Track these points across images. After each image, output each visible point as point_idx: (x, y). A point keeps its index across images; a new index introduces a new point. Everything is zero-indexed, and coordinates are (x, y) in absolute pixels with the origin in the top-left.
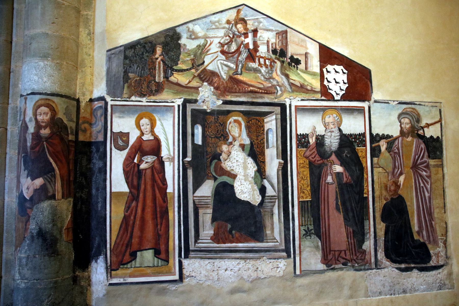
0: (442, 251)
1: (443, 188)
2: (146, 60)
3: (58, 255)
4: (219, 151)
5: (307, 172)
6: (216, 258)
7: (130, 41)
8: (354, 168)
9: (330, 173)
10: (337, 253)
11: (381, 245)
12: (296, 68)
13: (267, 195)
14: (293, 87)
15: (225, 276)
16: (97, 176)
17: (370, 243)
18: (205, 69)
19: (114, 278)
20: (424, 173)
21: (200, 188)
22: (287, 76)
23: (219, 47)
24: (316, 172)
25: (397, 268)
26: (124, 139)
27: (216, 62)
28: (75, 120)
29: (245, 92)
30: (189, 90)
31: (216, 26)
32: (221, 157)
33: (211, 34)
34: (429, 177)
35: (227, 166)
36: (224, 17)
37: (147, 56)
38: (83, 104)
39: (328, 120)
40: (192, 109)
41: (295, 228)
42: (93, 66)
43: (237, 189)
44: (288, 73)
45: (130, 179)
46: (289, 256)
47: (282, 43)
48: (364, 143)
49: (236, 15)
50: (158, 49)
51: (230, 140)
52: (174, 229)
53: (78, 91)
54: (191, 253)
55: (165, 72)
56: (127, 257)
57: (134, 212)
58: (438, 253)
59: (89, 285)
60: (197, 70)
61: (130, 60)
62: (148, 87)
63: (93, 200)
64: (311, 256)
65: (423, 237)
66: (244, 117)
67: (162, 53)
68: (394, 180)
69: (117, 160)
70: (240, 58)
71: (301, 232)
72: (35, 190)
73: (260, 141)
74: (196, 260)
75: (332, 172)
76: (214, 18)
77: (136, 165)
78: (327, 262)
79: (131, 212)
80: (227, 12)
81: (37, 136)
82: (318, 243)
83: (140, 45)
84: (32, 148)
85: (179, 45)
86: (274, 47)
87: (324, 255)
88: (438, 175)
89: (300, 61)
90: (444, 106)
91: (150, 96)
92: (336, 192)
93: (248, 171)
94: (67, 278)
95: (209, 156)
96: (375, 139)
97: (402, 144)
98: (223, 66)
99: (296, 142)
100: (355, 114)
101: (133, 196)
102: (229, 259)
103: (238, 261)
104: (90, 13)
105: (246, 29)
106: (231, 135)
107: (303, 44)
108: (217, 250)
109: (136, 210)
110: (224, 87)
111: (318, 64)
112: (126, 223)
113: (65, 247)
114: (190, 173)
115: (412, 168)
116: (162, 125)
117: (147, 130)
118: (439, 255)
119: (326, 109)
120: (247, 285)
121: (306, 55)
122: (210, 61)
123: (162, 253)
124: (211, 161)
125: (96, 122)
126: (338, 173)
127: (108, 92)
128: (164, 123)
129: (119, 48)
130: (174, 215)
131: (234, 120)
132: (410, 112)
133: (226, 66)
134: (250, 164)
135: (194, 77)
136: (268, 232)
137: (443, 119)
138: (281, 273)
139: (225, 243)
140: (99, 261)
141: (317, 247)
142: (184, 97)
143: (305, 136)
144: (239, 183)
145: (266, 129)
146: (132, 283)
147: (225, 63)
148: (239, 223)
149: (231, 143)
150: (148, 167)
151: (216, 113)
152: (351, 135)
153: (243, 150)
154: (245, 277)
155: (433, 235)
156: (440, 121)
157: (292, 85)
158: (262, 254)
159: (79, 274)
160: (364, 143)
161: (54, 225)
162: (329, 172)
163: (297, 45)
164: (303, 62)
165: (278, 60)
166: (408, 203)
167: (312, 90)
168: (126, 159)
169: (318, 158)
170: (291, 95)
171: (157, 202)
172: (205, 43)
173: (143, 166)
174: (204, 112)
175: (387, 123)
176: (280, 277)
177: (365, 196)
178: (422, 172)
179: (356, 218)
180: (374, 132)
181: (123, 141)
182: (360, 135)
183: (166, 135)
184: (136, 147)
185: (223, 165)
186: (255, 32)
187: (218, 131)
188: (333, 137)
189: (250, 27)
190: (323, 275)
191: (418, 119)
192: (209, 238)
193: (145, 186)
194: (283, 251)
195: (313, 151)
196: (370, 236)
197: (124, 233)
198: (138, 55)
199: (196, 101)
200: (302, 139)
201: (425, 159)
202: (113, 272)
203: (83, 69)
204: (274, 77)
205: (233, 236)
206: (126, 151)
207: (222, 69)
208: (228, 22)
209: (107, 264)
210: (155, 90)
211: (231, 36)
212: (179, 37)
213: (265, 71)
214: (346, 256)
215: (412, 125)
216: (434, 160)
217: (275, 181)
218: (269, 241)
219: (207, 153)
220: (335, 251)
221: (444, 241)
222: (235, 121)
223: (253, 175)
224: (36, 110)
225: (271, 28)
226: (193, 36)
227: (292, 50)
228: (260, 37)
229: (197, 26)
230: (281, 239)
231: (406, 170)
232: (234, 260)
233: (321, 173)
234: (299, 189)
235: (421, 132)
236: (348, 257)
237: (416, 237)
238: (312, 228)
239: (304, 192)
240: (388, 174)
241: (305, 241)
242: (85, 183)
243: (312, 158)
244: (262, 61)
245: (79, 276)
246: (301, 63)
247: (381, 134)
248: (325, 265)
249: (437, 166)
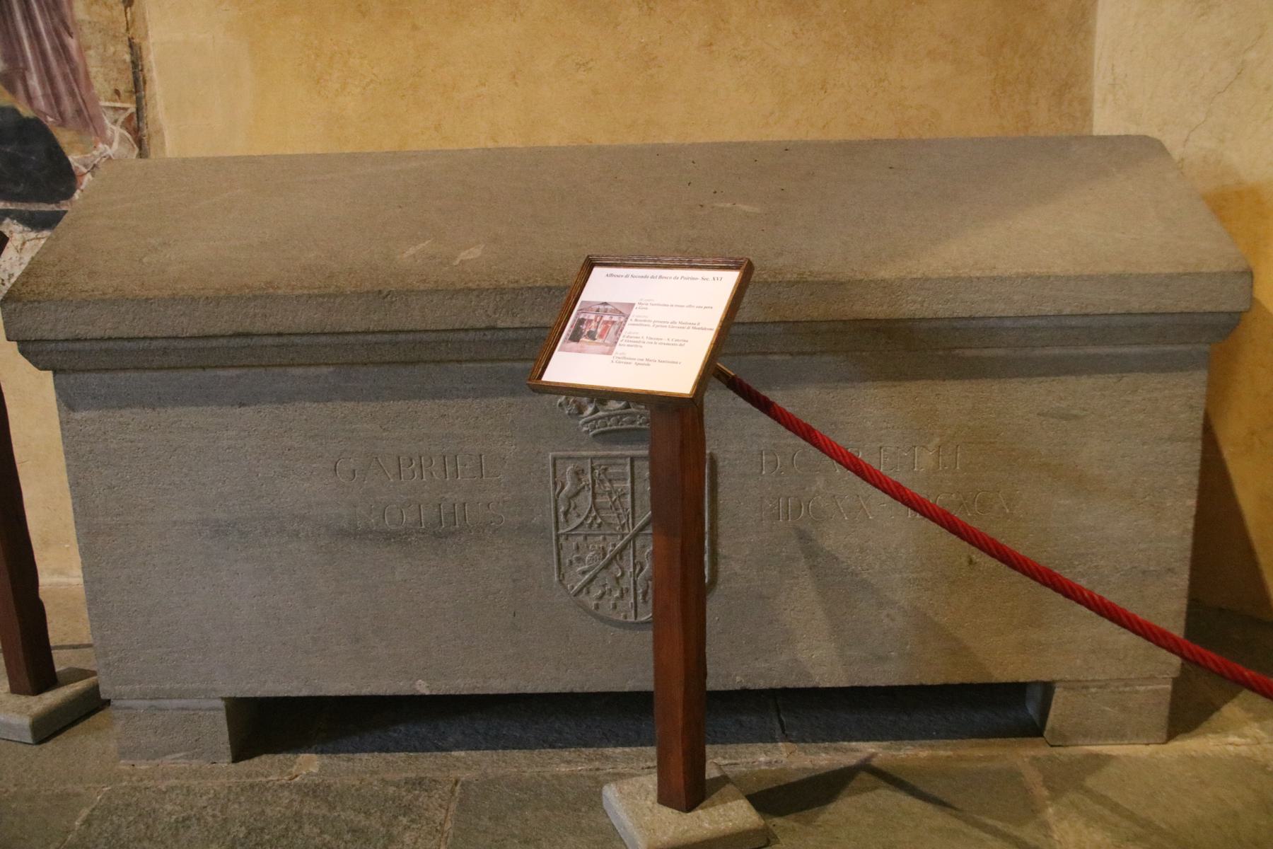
65: (30, 99)
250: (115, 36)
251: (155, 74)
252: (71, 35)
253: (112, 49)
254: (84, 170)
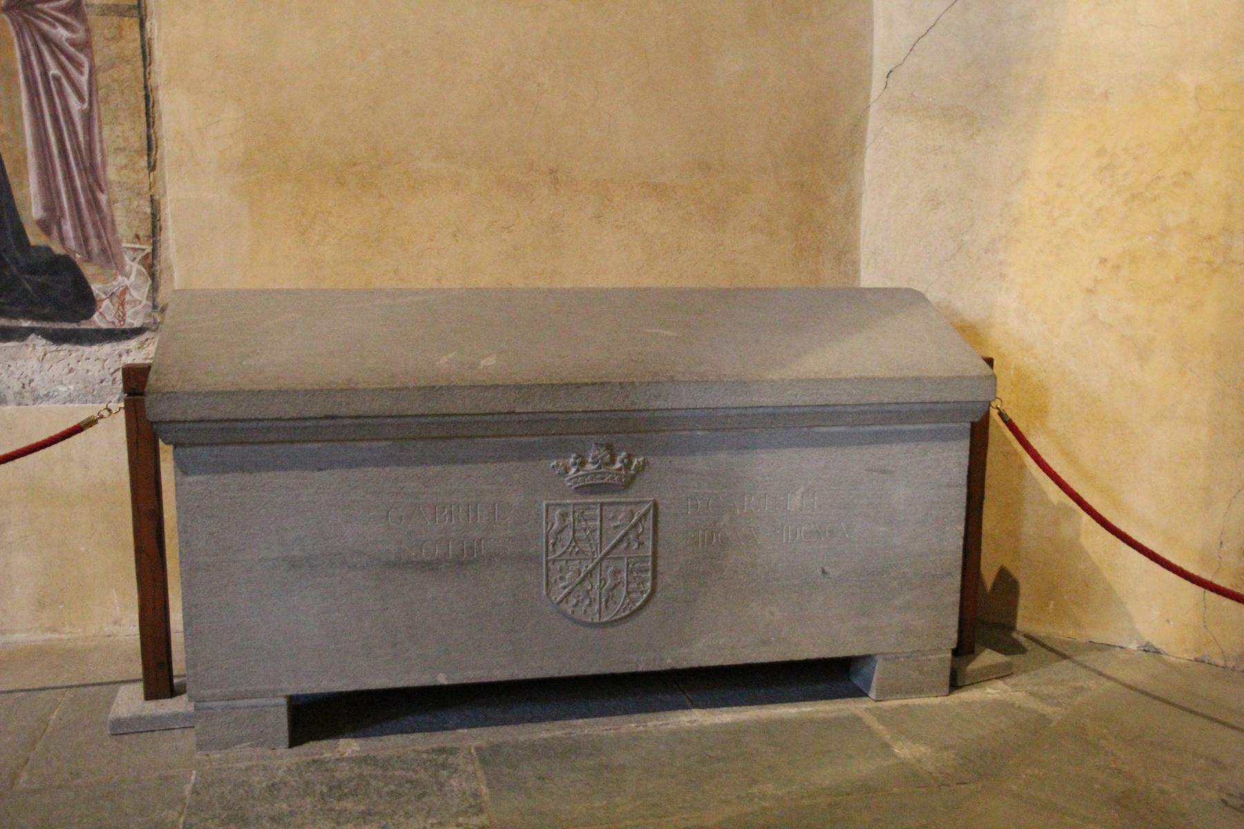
0: (137, 288)
1: (146, 87)
20: (62, 33)
34: (85, 46)
65: (62, 240)
88: (122, 44)
118: (127, 297)
155: (99, 237)
178: (54, 26)
221: (146, 257)
237: (35, 238)
250: (139, 194)
251: (170, 223)
252: (102, 191)
253: (136, 203)
254: (104, 296)
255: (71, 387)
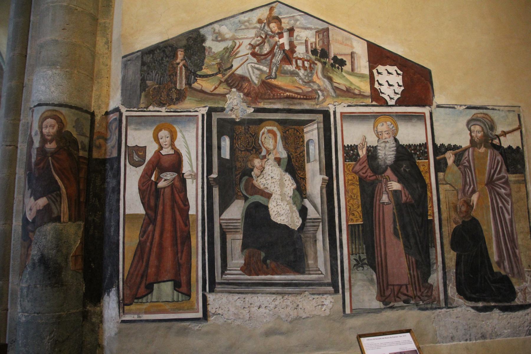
1: (528, 208)
2: (166, 66)
3: (62, 285)
4: (250, 166)
5: (357, 190)
6: (247, 293)
7: (148, 46)
8: (415, 185)
9: (386, 191)
10: (396, 288)
11: (451, 279)
12: (340, 70)
13: (308, 217)
14: (338, 92)
15: (259, 315)
16: (110, 197)
17: (438, 275)
18: (233, 73)
19: (127, 314)
20: (503, 191)
21: (228, 210)
22: (330, 79)
23: (249, 49)
24: (368, 191)
25: (473, 308)
26: (140, 154)
27: (246, 65)
28: (88, 135)
29: (280, 98)
30: (215, 97)
31: (246, 26)
32: (253, 173)
33: (240, 35)
34: (509, 195)
35: (260, 184)
36: (255, 16)
37: (167, 62)
38: (98, 118)
39: (380, 128)
40: (218, 119)
41: (344, 257)
42: (110, 76)
43: (273, 211)
44: (331, 75)
45: (146, 199)
46: (336, 291)
47: (323, 42)
48: (426, 155)
49: (268, 13)
50: (179, 53)
51: (264, 153)
52: (197, 257)
53: (93, 104)
54: (217, 286)
55: (187, 78)
56: (142, 290)
57: (150, 237)
58: (525, 289)
59: (102, 322)
60: (224, 75)
61: (148, 66)
62: (168, 95)
63: (106, 224)
64: (364, 292)
65: (504, 268)
66: (279, 127)
67: (184, 57)
68: (465, 199)
69: (132, 178)
70: (273, 60)
71: (352, 262)
72: (38, 212)
73: (299, 154)
74: (223, 294)
75: (387, 190)
76: (243, 18)
77: (154, 183)
78: (384, 298)
79: (148, 237)
80: (258, 10)
81: (42, 150)
82: (372, 276)
83: (159, 50)
84: (37, 164)
85: (204, 48)
86: (314, 46)
87: (381, 291)
89: (345, 61)
90: (523, 110)
91: (170, 105)
92: (394, 214)
93: (285, 189)
94: (74, 313)
95: (238, 172)
96: (439, 150)
97: (473, 155)
98: (254, 70)
99: (343, 155)
100: (414, 121)
101: (149, 218)
102: (263, 293)
103: (274, 296)
104: (108, 21)
105: (280, 28)
106: (264, 147)
107: (348, 43)
108: (249, 283)
109: (153, 235)
110: (255, 93)
111: (367, 64)
112: (141, 250)
113: (73, 277)
114: (216, 192)
115: (486, 185)
116: (184, 138)
117: (166, 143)
118: (527, 291)
119: (378, 116)
120: (285, 326)
121: (352, 54)
122: (239, 65)
123: (183, 286)
124: (241, 178)
125: (111, 136)
126: (395, 191)
127: (123, 102)
128: (186, 135)
129: (136, 54)
130: (197, 241)
131: (268, 130)
132: (481, 118)
133: (258, 69)
134: (287, 181)
135: (221, 82)
136: (311, 262)
137: (523, 126)
138: (328, 312)
139: (258, 275)
140: (111, 294)
141: (372, 281)
142: (209, 106)
143: (354, 148)
144: (274, 204)
145: (306, 140)
146: (147, 321)
147: (257, 66)
148: (276, 251)
149: (264, 157)
150: (167, 185)
151: (246, 122)
152: (410, 146)
153: (279, 165)
154: (283, 316)
155: (517, 267)
156: (520, 128)
157: (336, 89)
158: (303, 289)
159: (90, 309)
160: (426, 155)
161: (58, 251)
162: (384, 190)
163: (341, 44)
164: (348, 63)
165: (319, 61)
166: (484, 228)
167: (360, 95)
168: (142, 177)
169: (369, 173)
170: (335, 100)
171: (178, 226)
172: (234, 45)
173: (161, 184)
174: (232, 122)
175: (453, 132)
176: (325, 317)
177: (430, 218)
178: (500, 189)
179: (420, 246)
180: (438, 143)
181: (139, 156)
182: (420, 145)
183: (188, 148)
184: (153, 162)
185: (255, 182)
186: (291, 31)
187: (249, 143)
188: (387, 148)
189: (286, 25)
190: (379, 315)
191: (492, 126)
192: (239, 269)
193: (164, 208)
194: (328, 285)
195: (364, 165)
196: (437, 266)
197: (138, 262)
198: (157, 60)
199: (223, 110)
200: (350, 150)
201: (503, 174)
202: (126, 308)
203: (100, 80)
204: (315, 80)
205: (267, 266)
206: (143, 167)
207: (254, 73)
208: (260, 21)
209: (119, 297)
210: (176, 98)
211: (264, 37)
212: (203, 39)
213: (304, 74)
214: (407, 291)
215: (484, 133)
216: (514, 175)
217: (318, 201)
218: (311, 272)
219: (236, 169)
220: (393, 285)
222: (269, 131)
223: (291, 193)
224: (42, 123)
225: (309, 26)
226: (219, 38)
227: (335, 50)
228: (297, 36)
229: (224, 27)
230: (326, 270)
231: (479, 187)
232: (269, 295)
233: (375, 190)
234: (348, 210)
235: (496, 142)
236: (410, 293)
237: (496, 269)
238: (365, 257)
239: (353, 214)
240: (458, 193)
241: (356, 273)
242: (98, 205)
243: (363, 173)
244: (300, 63)
245: (91, 311)
246: (346, 64)
247: (446, 145)
248: (381, 303)
249: (518, 182)
255: (509, 330)
